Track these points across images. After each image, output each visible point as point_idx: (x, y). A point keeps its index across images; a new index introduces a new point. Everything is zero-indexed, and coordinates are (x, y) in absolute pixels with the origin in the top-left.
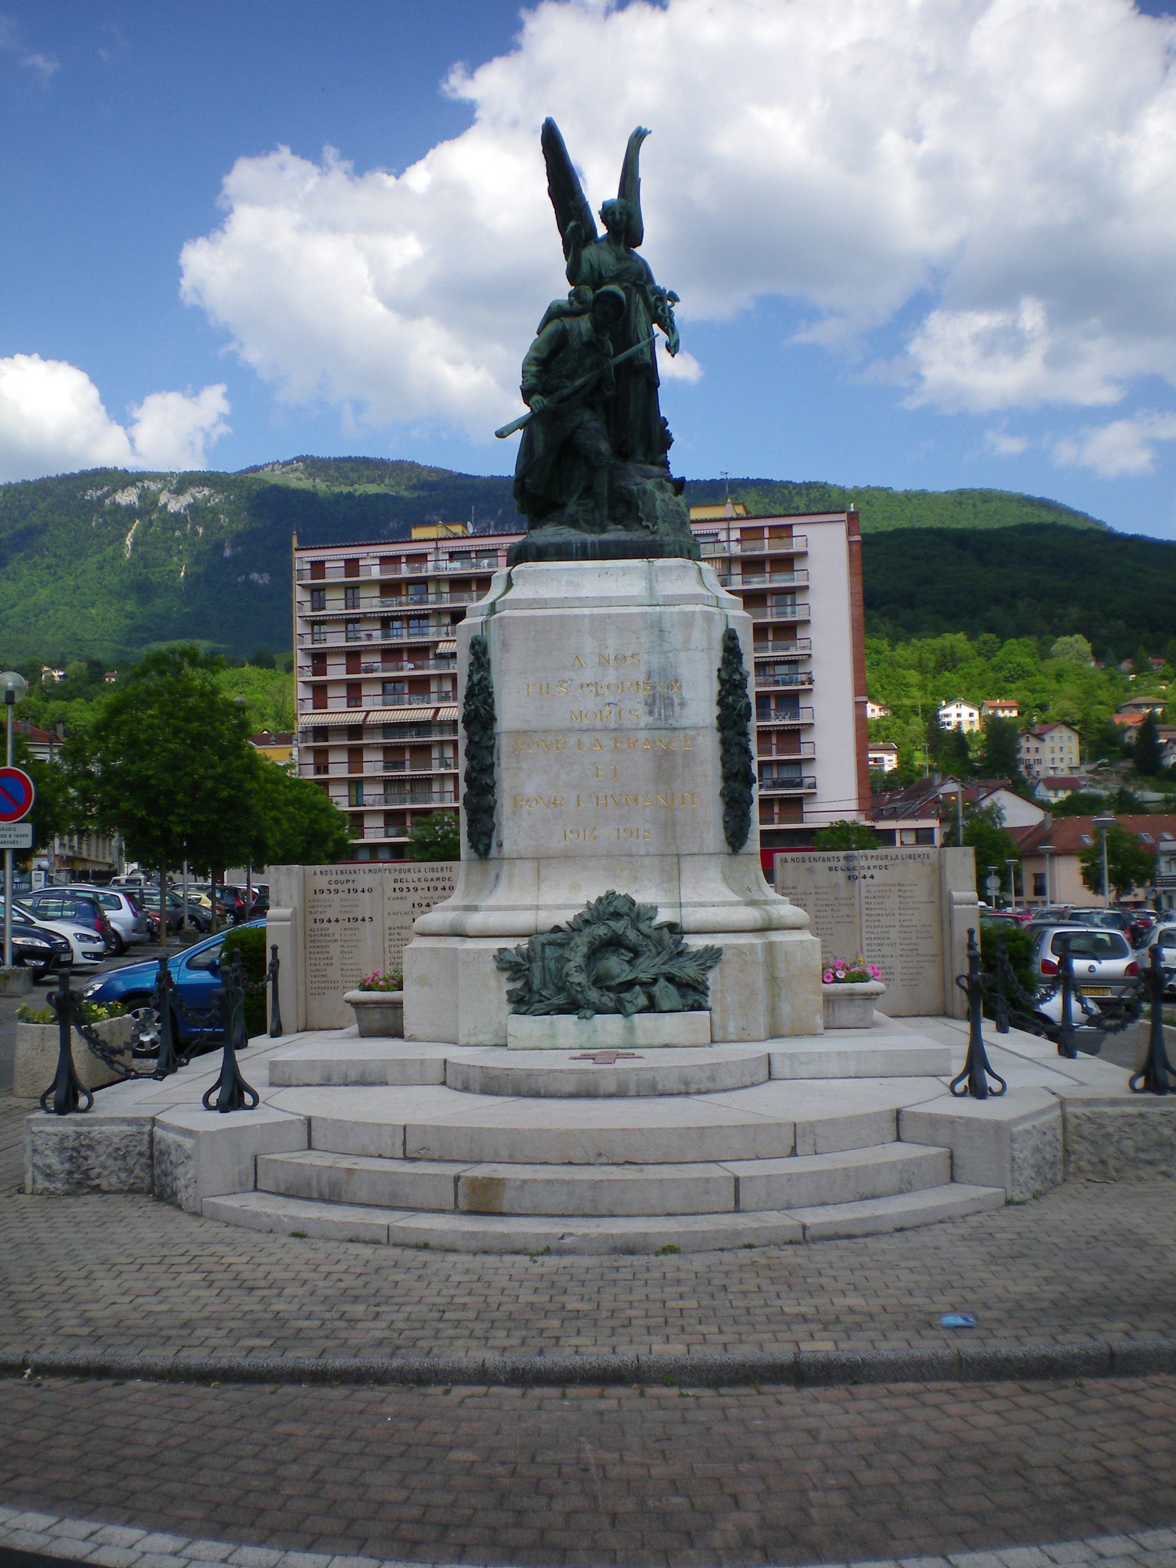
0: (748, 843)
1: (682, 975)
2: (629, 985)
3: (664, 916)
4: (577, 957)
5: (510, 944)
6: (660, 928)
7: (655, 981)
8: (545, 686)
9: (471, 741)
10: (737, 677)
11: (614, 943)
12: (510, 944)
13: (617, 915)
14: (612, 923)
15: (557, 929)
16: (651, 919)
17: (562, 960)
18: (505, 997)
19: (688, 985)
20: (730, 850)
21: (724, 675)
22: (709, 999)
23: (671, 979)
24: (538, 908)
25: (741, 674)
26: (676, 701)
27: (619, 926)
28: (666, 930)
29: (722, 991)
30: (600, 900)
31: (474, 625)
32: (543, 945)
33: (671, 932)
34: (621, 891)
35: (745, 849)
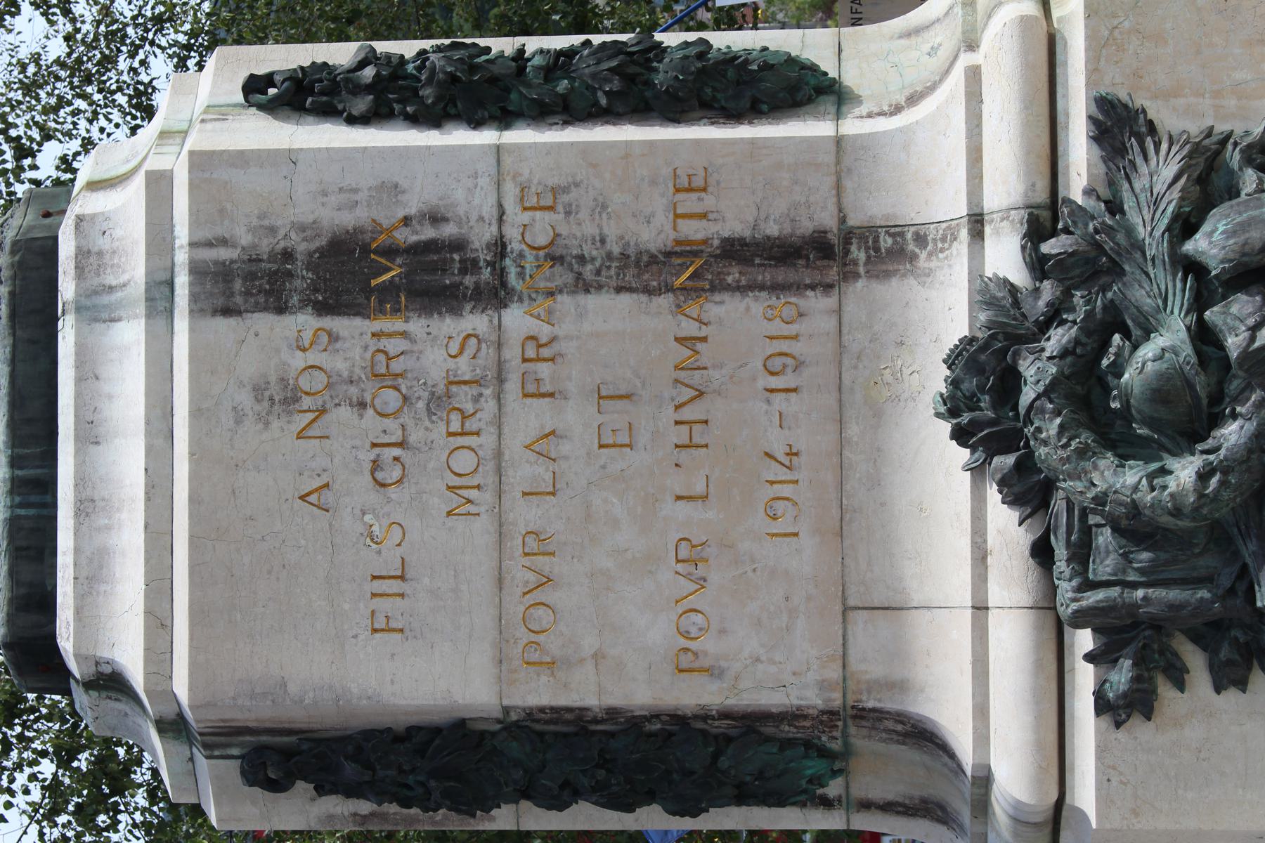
0: (809, 55)
1: (1175, 194)
2: (1204, 337)
3: (1005, 258)
4: (1123, 478)
5: (1084, 678)
6: (1039, 266)
7: (1193, 268)
8: (380, 586)
9: (527, 792)
10: (369, 72)
11: (1084, 386)
12: (1084, 678)
13: (1010, 382)
14: (1028, 395)
15: (1042, 552)
16: (1013, 289)
17: (1136, 527)
18: (1231, 697)
19: (1202, 180)
20: (828, 103)
21: (361, 105)
22: (1239, 131)
23: (1185, 226)
24: (980, 608)
25: (362, 64)
26: (428, 233)
27: (1035, 372)
28: (1049, 247)
29: (1217, 94)
30: (961, 436)
31: (217, 781)
32: (1089, 585)
33: (1054, 233)
34: (936, 379)
35: (828, 65)
